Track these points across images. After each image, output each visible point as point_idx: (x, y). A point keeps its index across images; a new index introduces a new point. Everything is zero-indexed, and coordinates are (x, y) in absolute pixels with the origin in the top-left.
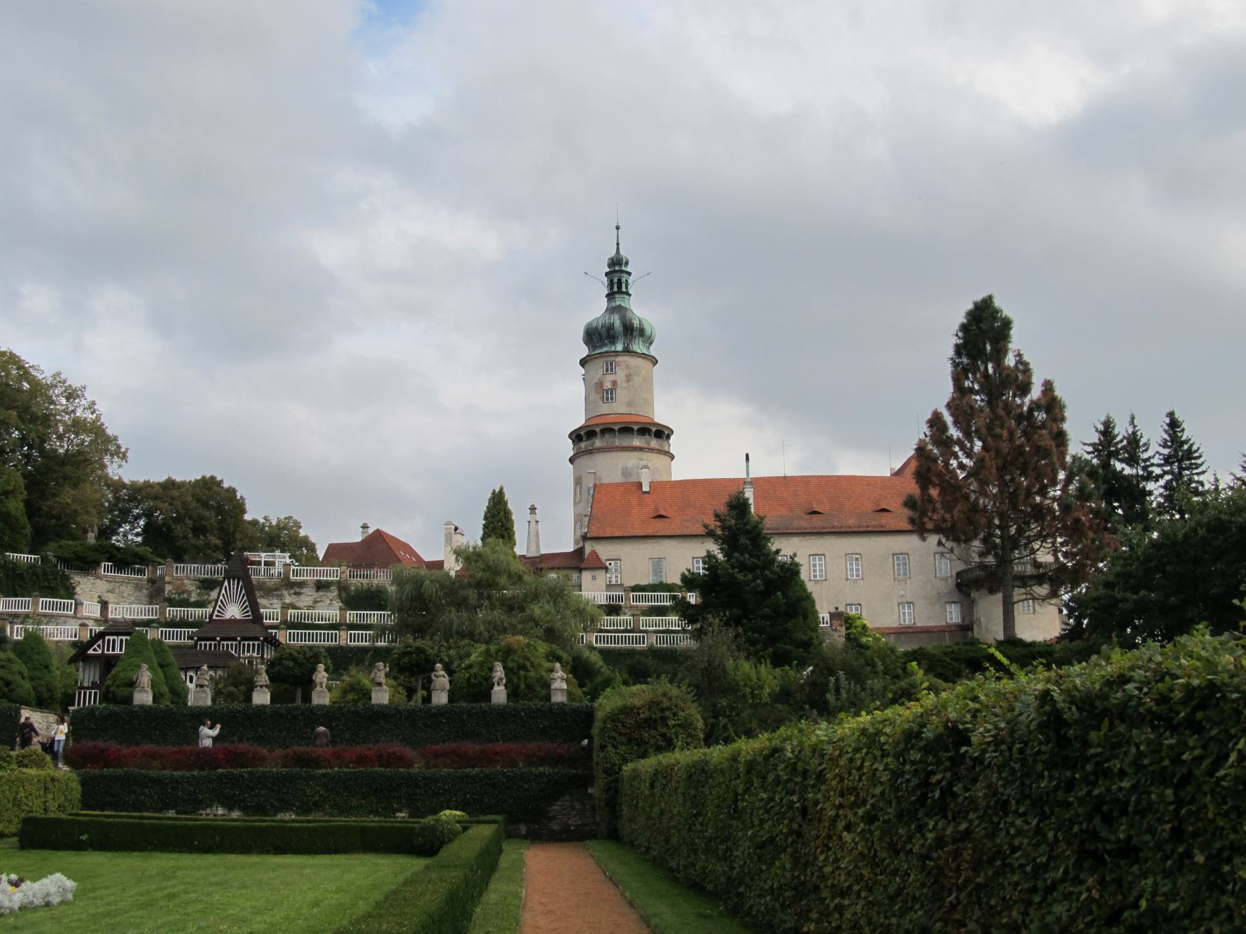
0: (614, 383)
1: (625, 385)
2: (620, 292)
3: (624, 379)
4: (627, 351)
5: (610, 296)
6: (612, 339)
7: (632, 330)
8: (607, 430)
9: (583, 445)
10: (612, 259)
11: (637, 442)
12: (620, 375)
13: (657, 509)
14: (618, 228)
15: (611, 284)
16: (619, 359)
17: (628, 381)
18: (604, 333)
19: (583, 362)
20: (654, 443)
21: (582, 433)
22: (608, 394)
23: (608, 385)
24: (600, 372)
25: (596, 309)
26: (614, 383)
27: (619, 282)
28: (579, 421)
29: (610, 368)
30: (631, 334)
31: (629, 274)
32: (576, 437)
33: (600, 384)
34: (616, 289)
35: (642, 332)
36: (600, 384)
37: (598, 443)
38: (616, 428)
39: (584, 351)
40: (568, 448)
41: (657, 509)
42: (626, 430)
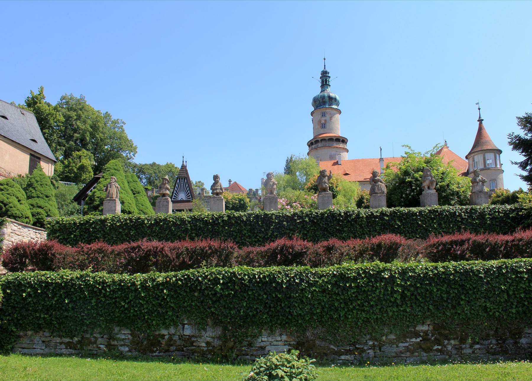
0: (325, 121)
6: (324, 104)
7: (332, 100)
8: (323, 140)
9: (313, 146)
10: (323, 71)
12: (328, 117)
13: (345, 171)
14: (325, 59)
15: (323, 82)
16: (327, 111)
18: (321, 101)
19: (312, 114)
20: (341, 145)
21: (313, 141)
22: (323, 126)
23: (323, 122)
24: (320, 116)
25: (317, 91)
26: (325, 121)
28: (311, 137)
29: (324, 115)
31: (330, 77)
32: (310, 144)
33: (320, 121)
34: (324, 83)
35: (335, 99)
36: (320, 121)
37: (320, 145)
39: (313, 109)
40: (307, 149)
41: (345, 171)
42: (331, 139)
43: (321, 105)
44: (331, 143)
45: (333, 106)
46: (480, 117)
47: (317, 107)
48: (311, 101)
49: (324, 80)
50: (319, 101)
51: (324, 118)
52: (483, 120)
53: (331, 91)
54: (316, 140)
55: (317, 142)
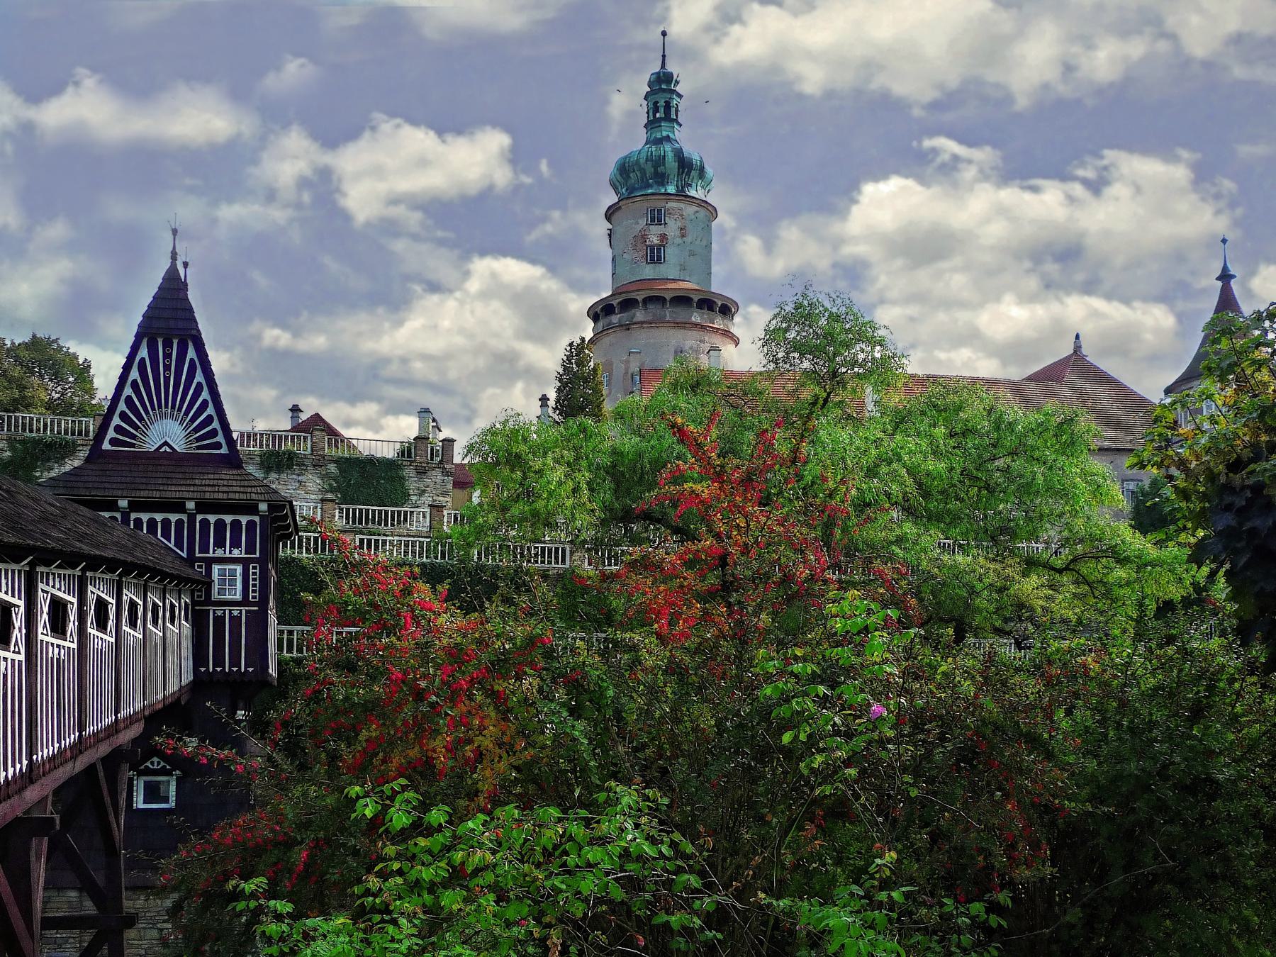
0: (663, 237)
1: (679, 241)
2: (667, 118)
3: (678, 233)
4: (682, 195)
5: (652, 124)
9: (615, 319)
11: (696, 317)
12: (672, 228)
16: (671, 205)
17: (683, 236)
18: (649, 170)
20: (719, 323)
21: (615, 303)
23: (655, 240)
24: (643, 222)
26: (663, 237)
27: (668, 106)
29: (657, 218)
30: (689, 174)
31: (680, 96)
36: (644, 237)
37: (639, 315)
38: (668, 296)
42: (682, 300)
43: (649, 186)
44: (681, 313)
45: (692, 193)
46: (1225, 268)
47: (631, 190)
48: (610, 168)
49: (662, 103)
50: (643, 171)
51: (655, 230)
52: (1233, 277)
53: (687, 138)
54: (624, 297)
55: (628, 304)
